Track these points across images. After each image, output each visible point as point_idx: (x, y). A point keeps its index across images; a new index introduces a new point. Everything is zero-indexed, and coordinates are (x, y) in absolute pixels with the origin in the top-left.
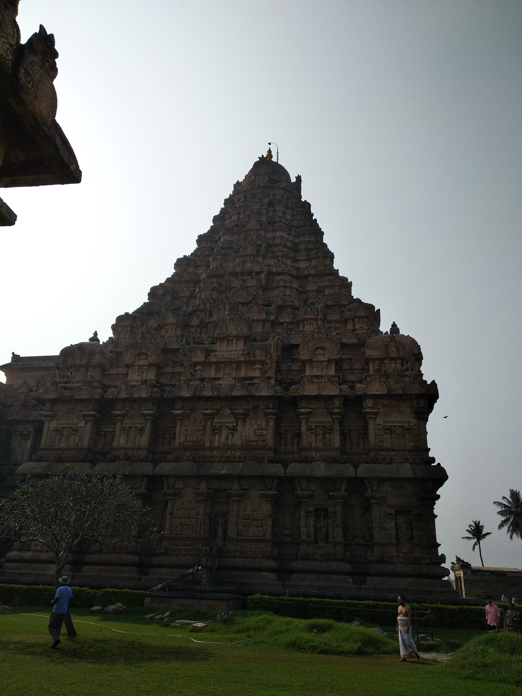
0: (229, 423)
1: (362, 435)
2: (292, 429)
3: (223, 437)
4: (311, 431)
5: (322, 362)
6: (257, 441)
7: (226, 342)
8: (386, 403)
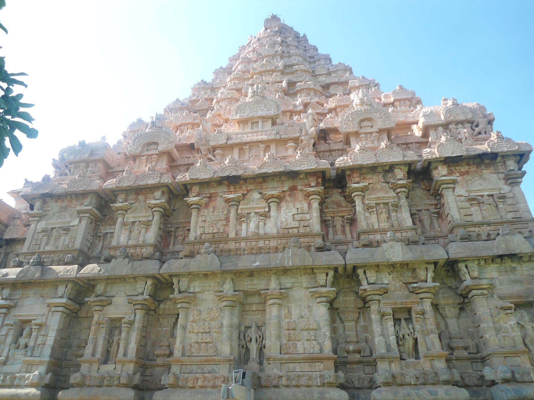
0: (259, 208)
1: (435, 215)
2: (341, 214)
3: (252, 225)
4: (370, 210)
5: (371, 133)
6: (298, 228)
7: (250, 124)
8: (463, 170)
